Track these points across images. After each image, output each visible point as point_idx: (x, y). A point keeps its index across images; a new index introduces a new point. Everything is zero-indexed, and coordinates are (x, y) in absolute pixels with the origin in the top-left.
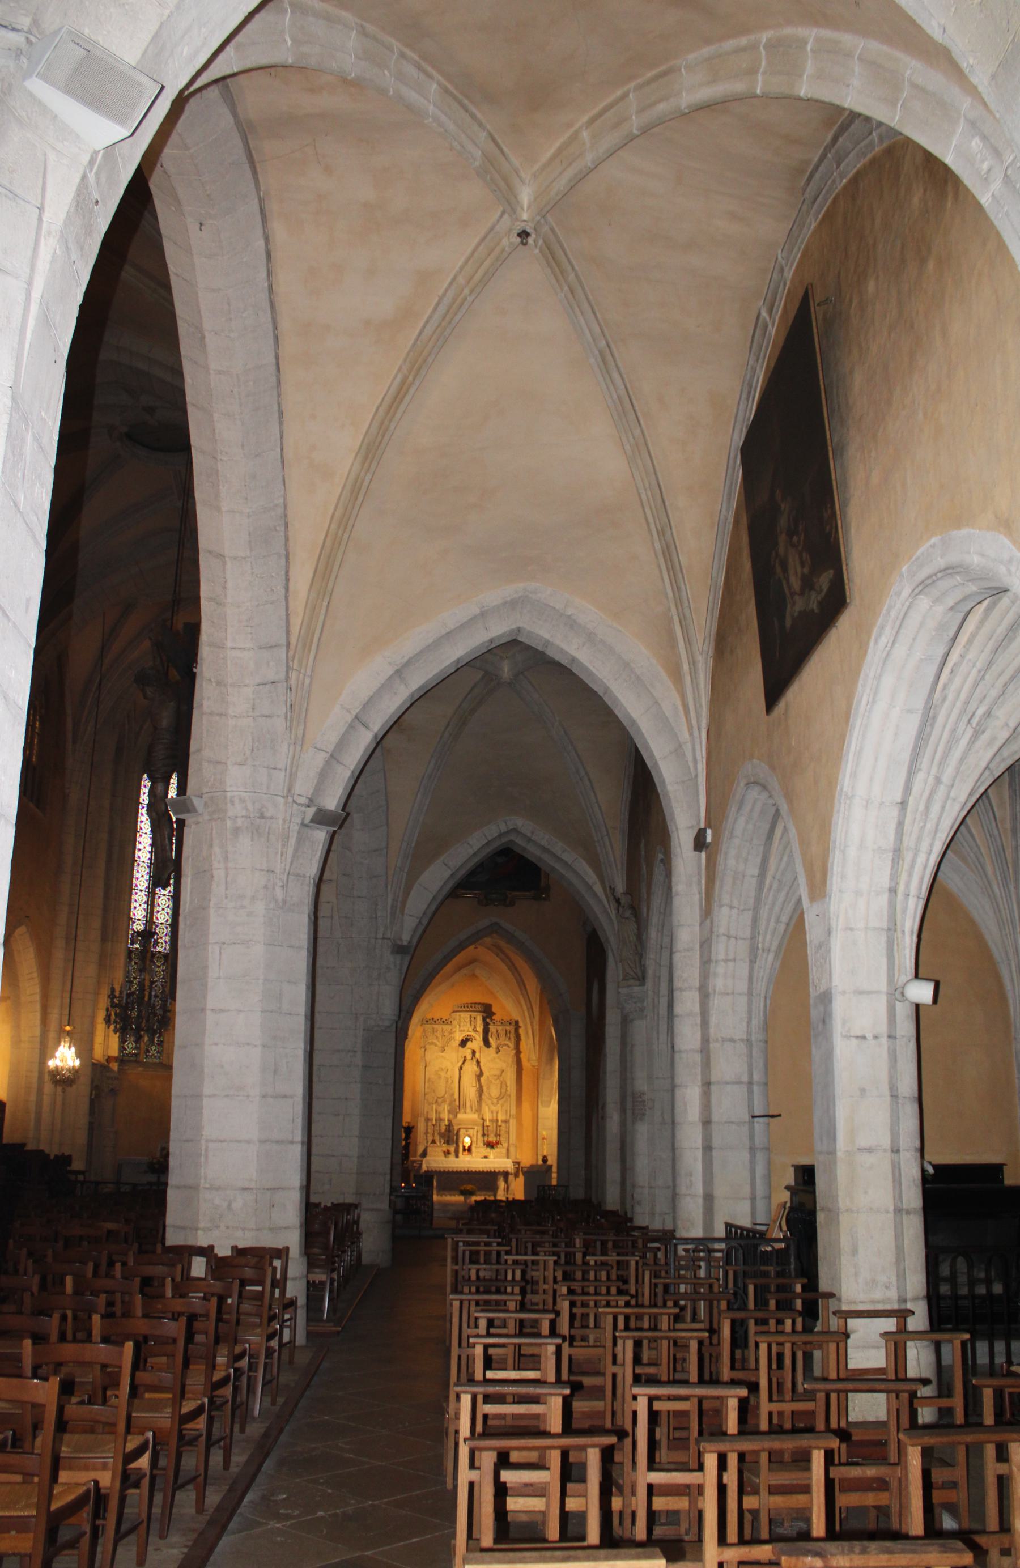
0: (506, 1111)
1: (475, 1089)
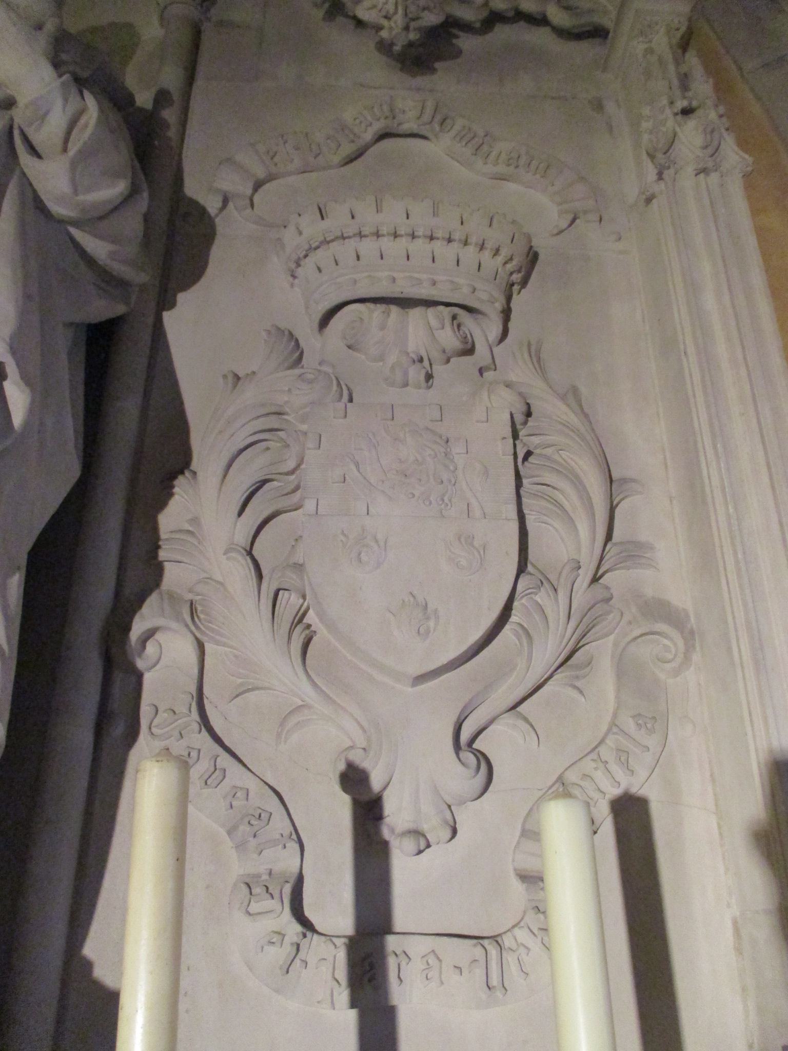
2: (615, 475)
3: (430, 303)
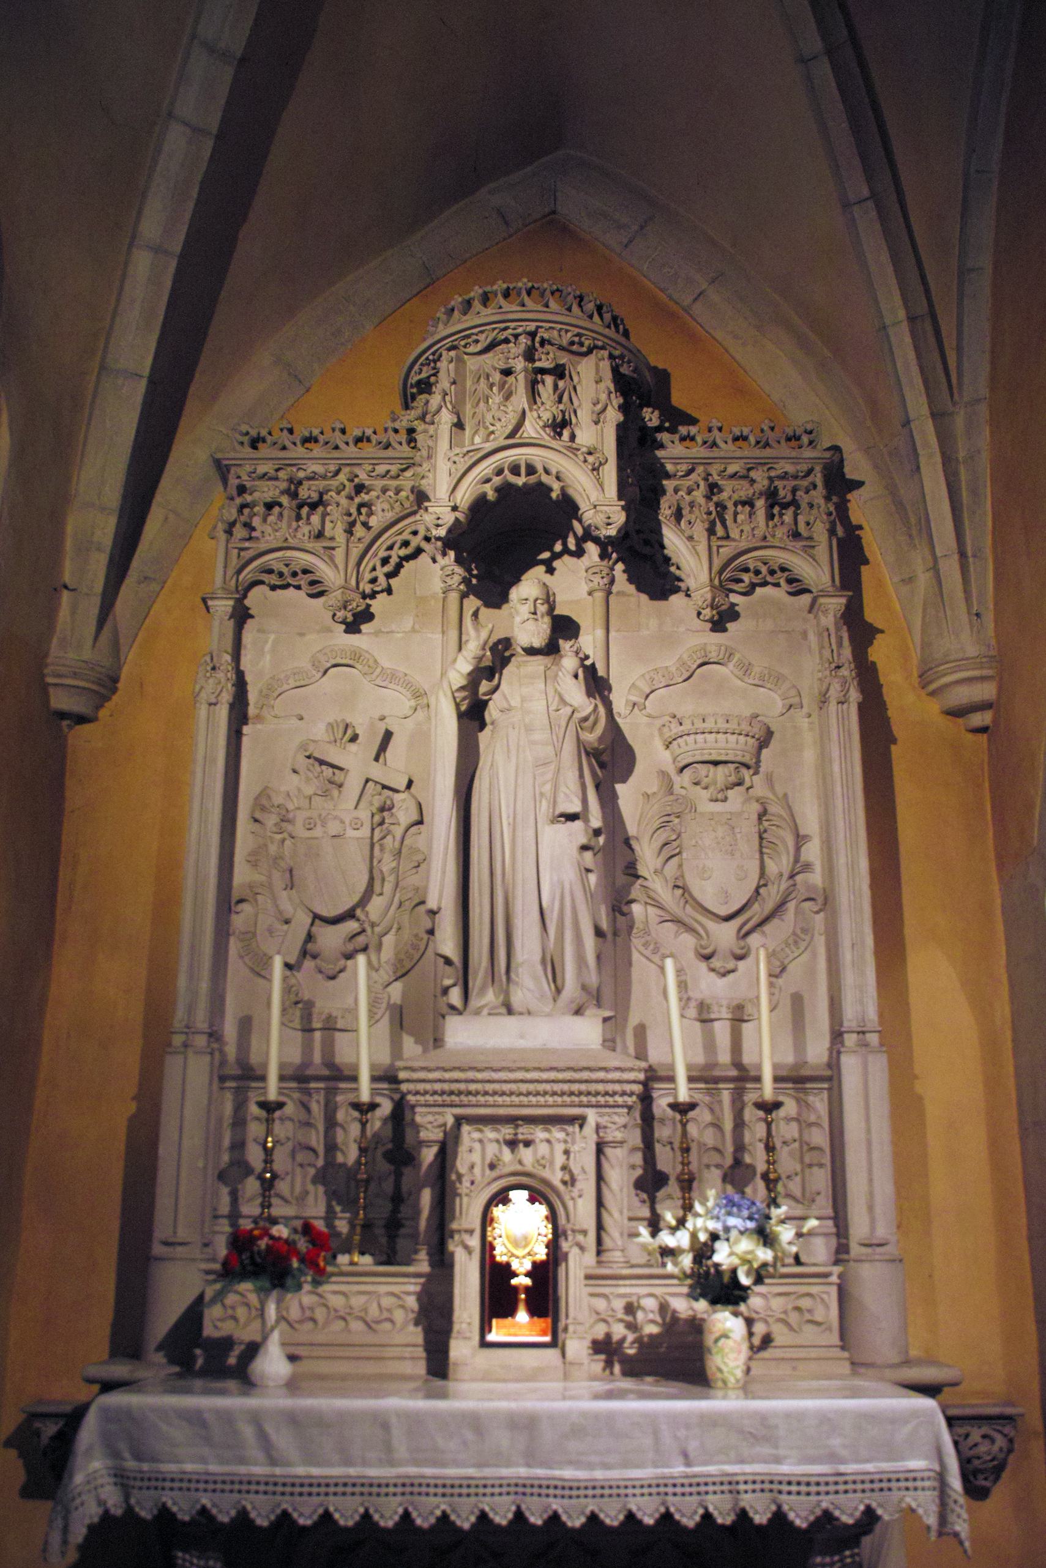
0: (797, 1002)
1: (577, 832)
3: (726, 762)
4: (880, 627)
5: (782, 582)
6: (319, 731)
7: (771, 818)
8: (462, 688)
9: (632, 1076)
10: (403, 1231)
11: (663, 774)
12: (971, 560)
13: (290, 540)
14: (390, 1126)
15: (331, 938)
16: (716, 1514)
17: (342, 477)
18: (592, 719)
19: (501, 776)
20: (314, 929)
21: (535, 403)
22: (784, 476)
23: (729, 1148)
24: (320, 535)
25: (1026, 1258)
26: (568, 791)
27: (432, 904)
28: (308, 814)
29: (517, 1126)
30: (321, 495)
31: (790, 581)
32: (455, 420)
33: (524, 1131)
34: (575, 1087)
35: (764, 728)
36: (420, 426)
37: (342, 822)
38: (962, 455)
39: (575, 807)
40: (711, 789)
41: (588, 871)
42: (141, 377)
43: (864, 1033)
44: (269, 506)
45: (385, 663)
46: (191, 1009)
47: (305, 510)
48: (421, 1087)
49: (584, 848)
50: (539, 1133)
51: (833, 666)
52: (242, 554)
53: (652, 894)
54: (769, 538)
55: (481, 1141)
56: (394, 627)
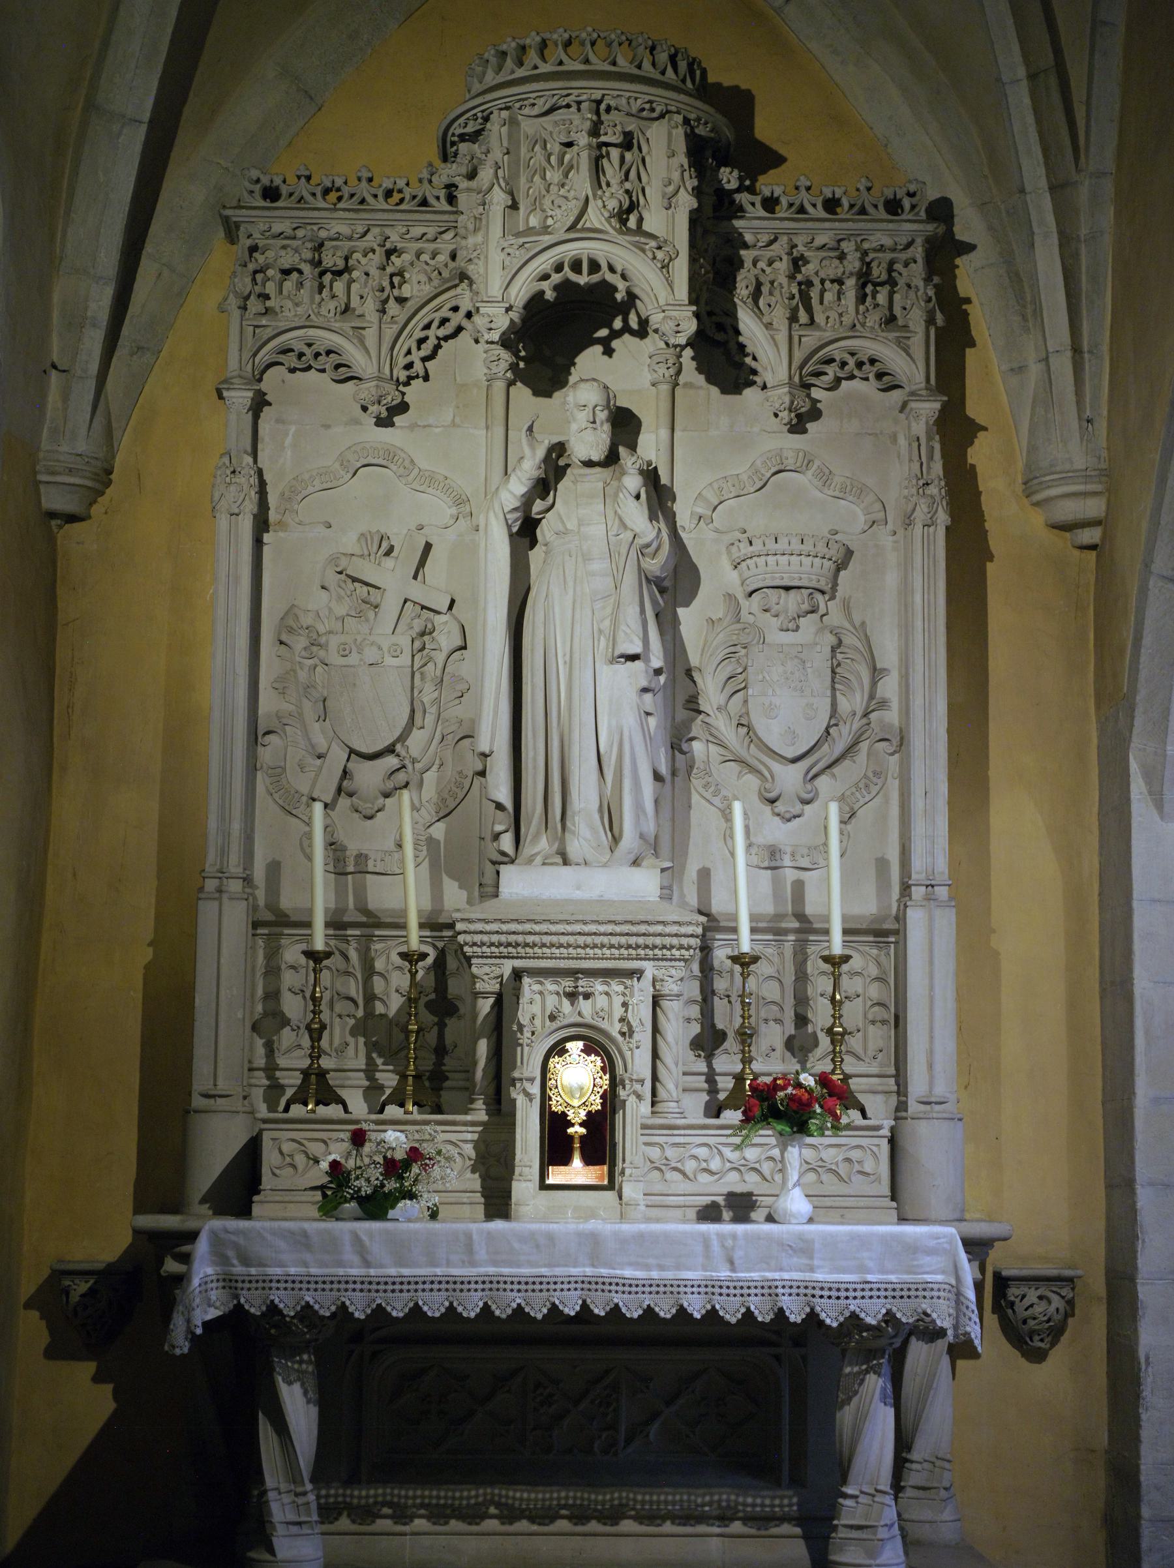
1: (637, 673)
2: (878, 666)
4: (983, 423)
5: (871, 376)
6: (349, 542)
7: (846, 650)
8: (515, 509)
9: (690, 930)
10: (447, 1084)
11: (730, 597)
12: (1086, 356)
13: (313, 316)
14: (432, 975)
15: (369, 776)
16: (756, 1313)
17: (369, 237)
18: (655, 545)
19: (557, 609)
20: (350, 765)
21: (600, 187)
22: (882, 249)
23: (789, 1003)
24: (347, 309)
25: (1100, 1122)
26: (628, 631)
27: (484, 747)
28: (343, 638)
29: (577, 979)
30: (347, 259)
31: (880, 376)
32: (510, 203)
33: (583, 984)
34: (632, 940)
35: (842, 550)
36: (463, 184)
37: (380, 648)
38: (1084, 231)
39: (636, 648)
40: (781, 618)
41: (648, 714)
42: (140, 122)
43: (933, 886)
44: (286, 272)
45: (422, 463)
46: (224, 852)
47: (328, 277)
48: (477, 938)
49: (645, 690)
50: (599, 986)
51: (921, 483)
52: (257, 331)
53: (714, 731)
54: (858, 326)
55: (541, 993)
56: (431, 421)
